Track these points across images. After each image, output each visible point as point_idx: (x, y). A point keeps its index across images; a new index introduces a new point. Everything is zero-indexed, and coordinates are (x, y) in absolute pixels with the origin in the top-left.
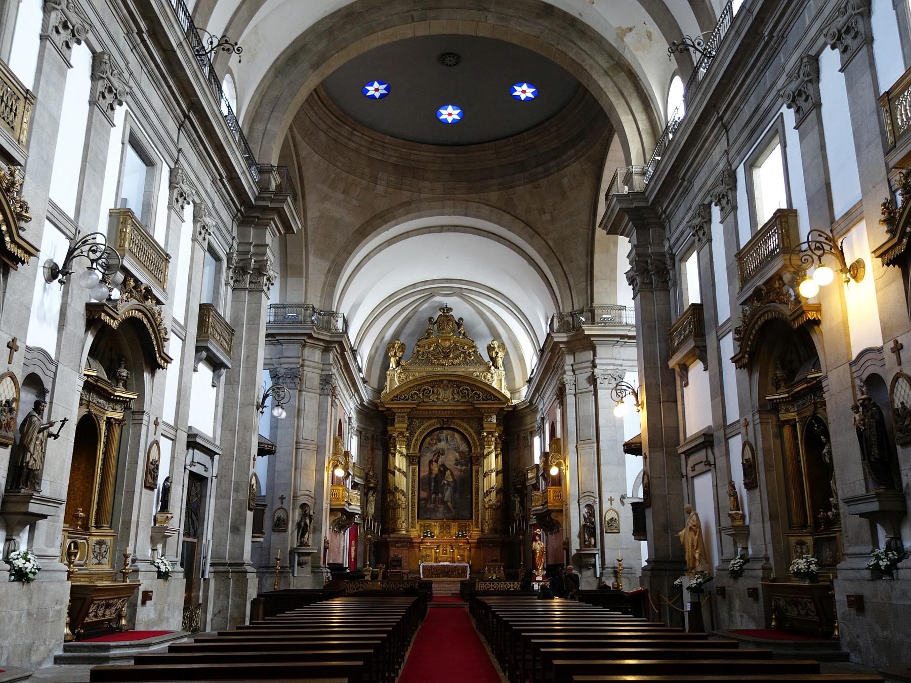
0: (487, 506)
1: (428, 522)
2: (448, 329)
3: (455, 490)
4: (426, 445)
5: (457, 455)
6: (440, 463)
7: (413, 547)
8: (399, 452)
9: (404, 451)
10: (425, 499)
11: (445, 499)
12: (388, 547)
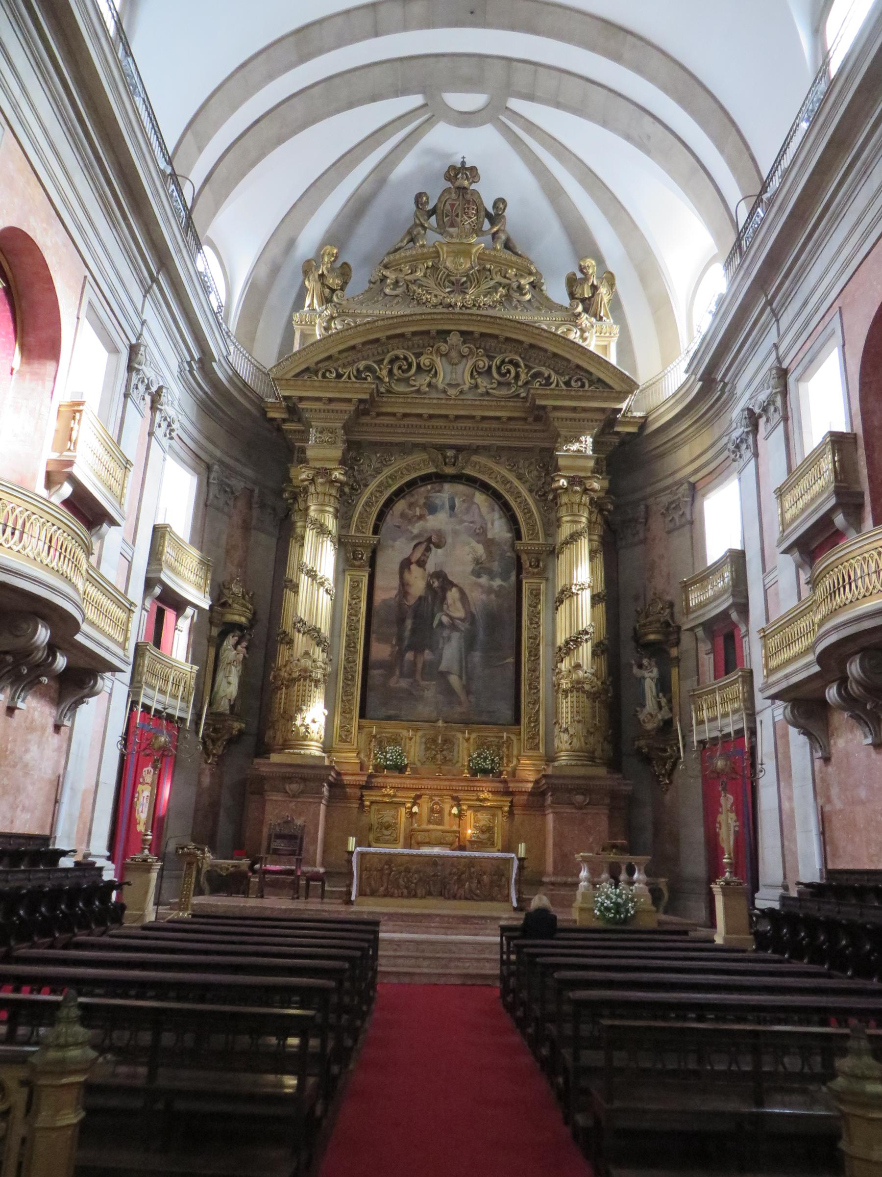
0: (565, 684)
1: (391, 728)
2: (468, 222)
3: (470, 643)
4: (392, 519)
5: (480, 549)
6: (431, 567)
7: (346, 798)
8: (314, 522)
9: (331, 523)
10: (381, 665)
11: (443, 667)
12: (261, 792)
